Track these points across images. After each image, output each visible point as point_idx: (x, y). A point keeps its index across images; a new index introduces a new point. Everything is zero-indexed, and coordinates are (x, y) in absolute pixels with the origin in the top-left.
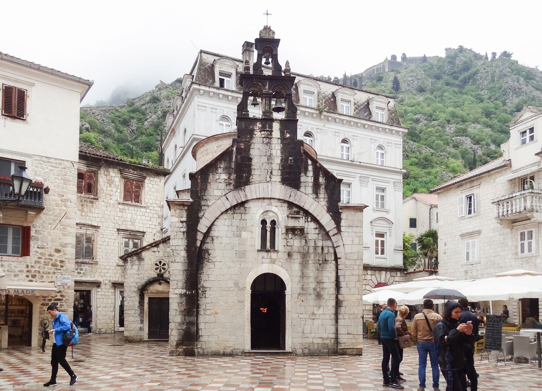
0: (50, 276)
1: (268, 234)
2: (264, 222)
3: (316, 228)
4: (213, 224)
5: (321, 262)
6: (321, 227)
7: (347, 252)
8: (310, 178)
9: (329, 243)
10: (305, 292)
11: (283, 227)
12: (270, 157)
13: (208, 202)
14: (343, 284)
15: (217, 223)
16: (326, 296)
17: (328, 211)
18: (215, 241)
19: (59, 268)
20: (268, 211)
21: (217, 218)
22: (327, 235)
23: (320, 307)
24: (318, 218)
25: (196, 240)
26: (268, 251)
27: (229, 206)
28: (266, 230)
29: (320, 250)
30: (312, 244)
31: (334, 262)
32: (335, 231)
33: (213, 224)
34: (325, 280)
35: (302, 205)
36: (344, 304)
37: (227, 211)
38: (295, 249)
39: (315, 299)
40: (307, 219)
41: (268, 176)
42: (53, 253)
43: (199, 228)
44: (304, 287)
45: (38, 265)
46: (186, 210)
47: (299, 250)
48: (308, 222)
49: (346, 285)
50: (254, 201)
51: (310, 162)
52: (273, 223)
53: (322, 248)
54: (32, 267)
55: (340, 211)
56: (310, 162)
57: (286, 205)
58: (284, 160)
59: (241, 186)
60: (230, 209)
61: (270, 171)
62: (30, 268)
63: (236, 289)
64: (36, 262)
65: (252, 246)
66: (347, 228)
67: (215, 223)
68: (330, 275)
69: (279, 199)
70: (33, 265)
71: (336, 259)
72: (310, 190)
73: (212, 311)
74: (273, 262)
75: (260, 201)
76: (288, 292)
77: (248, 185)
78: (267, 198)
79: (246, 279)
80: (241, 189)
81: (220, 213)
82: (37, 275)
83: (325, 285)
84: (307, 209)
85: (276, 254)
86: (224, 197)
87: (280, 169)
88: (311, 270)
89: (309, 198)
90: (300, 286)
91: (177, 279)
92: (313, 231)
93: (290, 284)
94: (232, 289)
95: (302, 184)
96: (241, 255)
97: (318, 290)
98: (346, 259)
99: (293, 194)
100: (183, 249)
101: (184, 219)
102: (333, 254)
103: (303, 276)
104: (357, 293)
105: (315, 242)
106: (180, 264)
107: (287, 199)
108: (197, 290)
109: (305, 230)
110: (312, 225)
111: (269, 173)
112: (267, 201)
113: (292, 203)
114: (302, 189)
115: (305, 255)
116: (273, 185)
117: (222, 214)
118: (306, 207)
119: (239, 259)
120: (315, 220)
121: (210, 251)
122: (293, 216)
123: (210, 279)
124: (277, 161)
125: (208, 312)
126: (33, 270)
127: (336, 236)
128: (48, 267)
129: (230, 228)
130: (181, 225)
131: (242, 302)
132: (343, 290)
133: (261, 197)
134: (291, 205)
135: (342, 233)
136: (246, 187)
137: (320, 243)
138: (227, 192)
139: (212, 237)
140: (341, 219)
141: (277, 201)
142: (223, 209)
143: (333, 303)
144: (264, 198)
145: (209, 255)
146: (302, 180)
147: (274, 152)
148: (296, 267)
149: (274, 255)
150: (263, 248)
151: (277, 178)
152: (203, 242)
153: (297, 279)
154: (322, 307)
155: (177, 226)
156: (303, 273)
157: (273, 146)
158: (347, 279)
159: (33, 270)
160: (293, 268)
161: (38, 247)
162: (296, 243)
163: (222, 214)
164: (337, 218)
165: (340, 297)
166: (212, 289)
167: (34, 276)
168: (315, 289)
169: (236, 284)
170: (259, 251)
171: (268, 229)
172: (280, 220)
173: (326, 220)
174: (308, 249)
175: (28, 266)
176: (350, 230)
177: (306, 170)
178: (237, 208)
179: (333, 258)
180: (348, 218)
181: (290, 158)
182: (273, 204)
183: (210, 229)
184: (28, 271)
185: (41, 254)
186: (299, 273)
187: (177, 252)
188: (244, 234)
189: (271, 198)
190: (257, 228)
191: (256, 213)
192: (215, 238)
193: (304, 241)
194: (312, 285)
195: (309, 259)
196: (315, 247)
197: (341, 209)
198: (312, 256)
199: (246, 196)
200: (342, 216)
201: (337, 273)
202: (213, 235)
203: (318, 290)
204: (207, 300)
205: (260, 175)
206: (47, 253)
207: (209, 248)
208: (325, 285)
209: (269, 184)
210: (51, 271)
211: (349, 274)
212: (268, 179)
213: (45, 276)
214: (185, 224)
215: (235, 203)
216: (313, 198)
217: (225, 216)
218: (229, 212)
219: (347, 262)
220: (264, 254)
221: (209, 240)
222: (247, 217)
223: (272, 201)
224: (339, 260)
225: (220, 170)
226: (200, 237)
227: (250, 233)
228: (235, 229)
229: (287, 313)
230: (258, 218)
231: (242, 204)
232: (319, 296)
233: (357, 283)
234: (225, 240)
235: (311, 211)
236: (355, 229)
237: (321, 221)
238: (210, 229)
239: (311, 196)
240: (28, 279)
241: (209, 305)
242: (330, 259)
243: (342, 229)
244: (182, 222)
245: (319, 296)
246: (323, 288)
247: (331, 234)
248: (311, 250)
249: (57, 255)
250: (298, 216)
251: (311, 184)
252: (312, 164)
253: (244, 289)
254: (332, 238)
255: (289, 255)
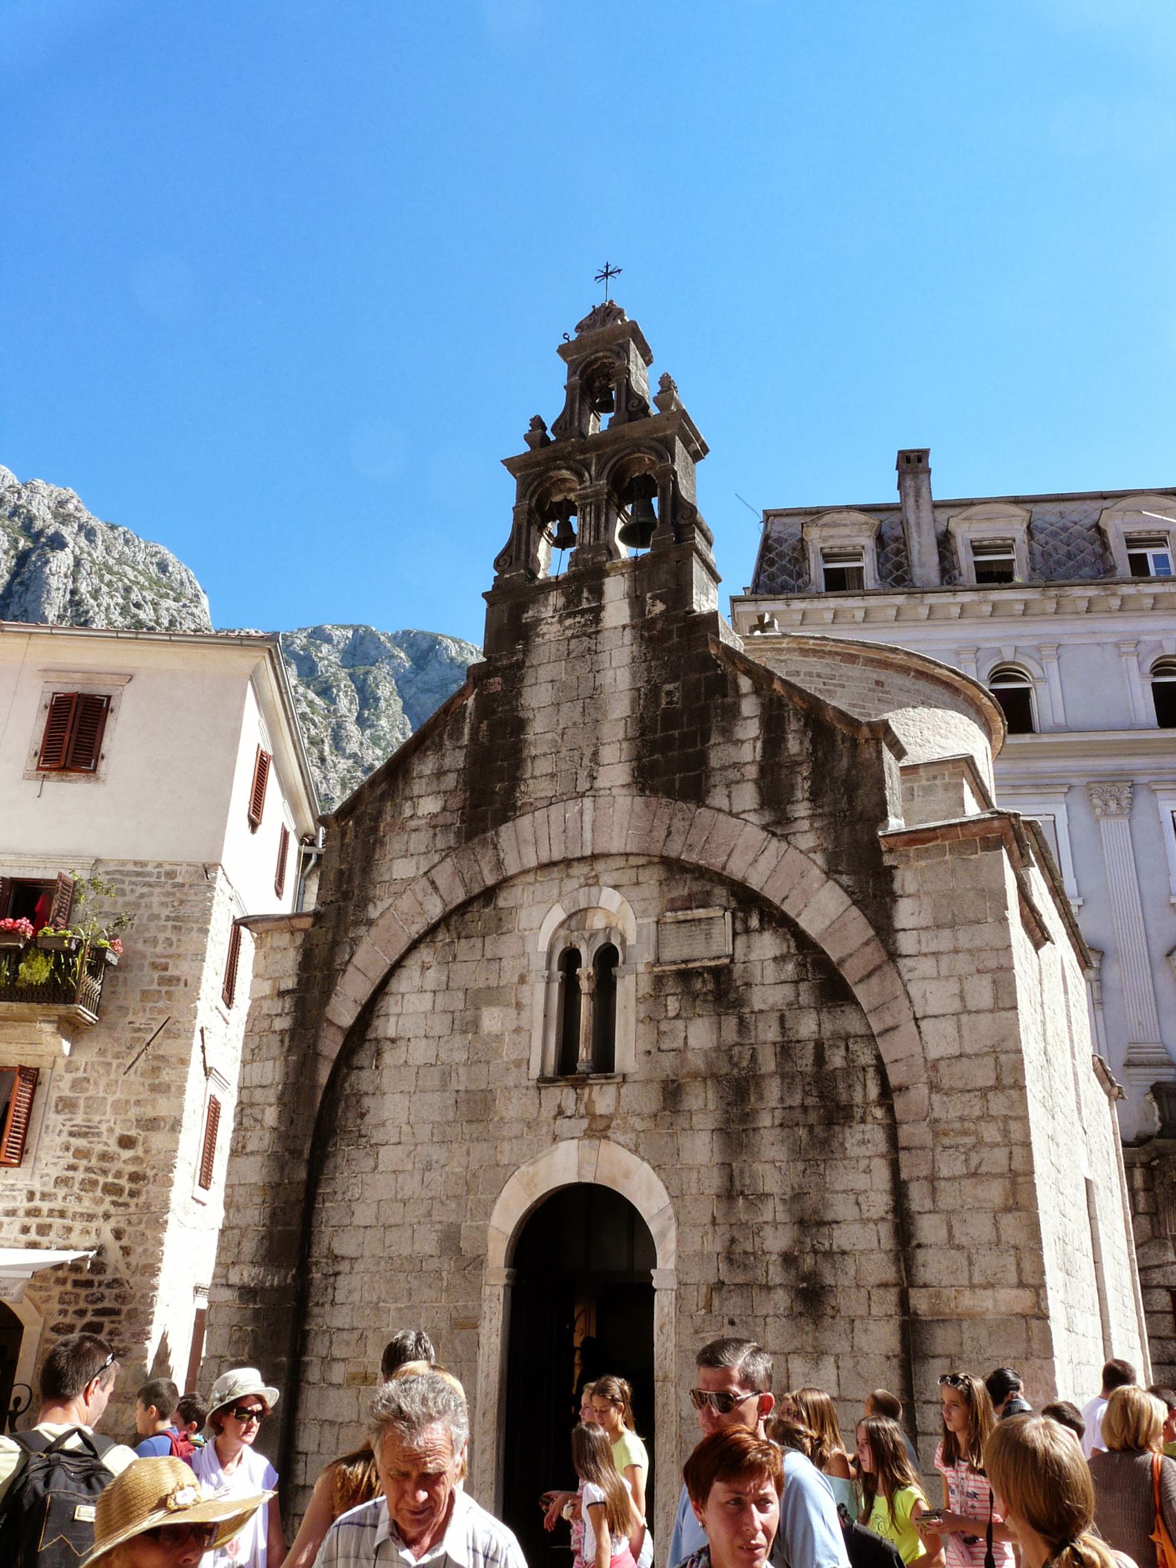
0: (94, 1225)
1: (586, 1006)
2: (570, 958)
3: (779, 960)
4: (381, 990)
5: (813, 1118)
6: (805, 947)
7: (933, 1054)
8: (747, 747)
9: (851, 1022)
10: (740, 1278)
11: (641, 968)
12: (593, 698)
13: (371, 907)
14: (929, 1229)
15: (404, 983)
16: (849, 1302)
17: (831, 872)
18: (388, 1058)
19: (124, 1198)
20: (585, 910)
21: (397, 965)
22: (832, 988)
23: (818, 1355)
24: (785, 908)
25: (317, 1055)
26: (579, 1083)
27: (435, 909)
28: (592, 995)
29: (805, 1061)
30: (769, 1032)
31: (879, 1113)
32: (874, 954)
33: (381, 990)
34: (842, 1208)
35: (716, 862)
36: (942, 1340)
37: (432, 931)
38: (697, 1062)
39: (791, 1316)
40: (745, 921)
41: (583, 774)
42: (113, 1148)
43: (330, 1012)
44: (738, 1249)
45: (61, 1192)
46: (298, 948)
47: (710, 1064)
48: (747, 931)
49: (943, 1233)
50: (530, 878)
51: (745, 684)
52: (607, 957)
53: (819, 1047)
54: (44, 1196)
55: (888, 860)
56: (745, 684)
57: (652, 876)
58: (647, 697)
59: (484, 831)
60: (445, 920)
61: (588, 752)
62: (37, 1203)
63: (447, 1266)
64: (60, 1181)
65: (518, 1064)
66: (924, 935)
67: (394, 986)
68: (860, 1181)
69: (627, 855)
70: (49, 1189)
71: (887, 1094)
72: (747, 796)
73: (352, 1369)
74: (599, 1129)
75: (556, 873)
76: (664, 1275)
77: (506, 820)
78: (581, 859)
79: (488, 1215)
80: (484, 843)
81: (403, 944)
82: (57, 1222)
83: (842, 1238)
84: (738, 875)
85: (611, 1090)
86: (424, 882)
87: (626, 739)
88: (772, 1165)
89: (749, 828)
90: (715, 1245)
91: (242, 1223)
92: (770, 973)
93: (672, 1234)
94: (433, 1264)
95: (716, 778)
96: (477, 1108)
97: (808, 1262)
98: (934, 1087)
99: (678, 824)
100: (273, 1100)
101: (290, 983)
102: (871, 1073)
103: (731, 1192)
104: (1013, 1278)
105: (782, 1019)
106: (259, 1158)
107: (656, 849)
108: (303, 1264)
109: (738, 969)
110: (767, 945)
111: (586, 762)
112: (580, 870)
113: (678, 860)
114: (718, 798)
115: (738, 1090)
116: (601, 801)
117: (414, 946)
118: (737, 868)
119: (467, 1128)
120: (777, 919)
121: (367, 1102)
122: (681, 915)
123: (359, 1220)
124: (619, 707)
125: (338, 1373)
126: (45, 1206)
127: (875, 980)
128: (91, 1194)
129: (440, 996)
130: (276, 1006)
131: (468, 1324)
132: (934, 1265)
133: (557, 856)
134: (673, 867)
135: (902, 963)
136: (503, 828)
137: (807, 1026)
138: (437, 858)
139: (377, 1040)
140: (894, 898)
141: (620, 862)
142: (417, 928)
143: (882, 1337)
144: (567, 862)
145: (362, 1116)
146: (714, 762)
147: (607, 678)
148: (700, 1148)
149: (603, 1099)
150: (566, 1068)
151: (615, 772)
152: (345, 1061)
153: (703, 1211)
154: (829, 1361)
155: (265, 1011)
156: (731, 1178)
157: (605, 657)
158: (948, 1197)
159: (45, 1206)
160: (686, 1157)
161: (71, 1134)
162: (700, 1035)
163: (414, 946)
164: (873, 890)
165: (920, 1302)
166: (359, 1267)
167: (43, 1230)
168: (789, 1260)
169: (450, 1240)
170: (544, 1081)
171: (585, 986)
172: (631, 940)
173: (824, 909)
174: (753, 1058)
175: (31, 1196)
176: (944, 940)
177: (732, 713)
178: (468, 916)
179: (873, 1091)
180: (928, 887)
181: (668, 687)
182: (606, 878)
183: (369, 1010)
184: (30, 1213)
185: (80, 1154)
186: (713, 1182)
187: (256, 1111)
188: (492, 1020)
189: (594, 857)
190: (540, 988)
191: (537, 923)
192: (387, 1046)
193: (731, 1022)
194: (777, 1241)
195: (759, 1106)
196: (785, 1050)
197: (890, 850)
198: (773, 1090)
199: (499, 864)
200: (897, 886)
201: (895, 1168)
202: (380, 1033)
203: (808, 1262)
204: (339, 1318)
205: (553, 776)
206: (99, 1148)
207: (364, 1087)
208: (842, 1238)
209: (588, 802)
210: (100, 1210)
211: (959, 1169)
212: (583, 785)
213: (78, 1226)
214: (288, 1003)
215: (460, 896)
216: (764, 828)
217: (425, 954)
218: (440, 937)
219: (948, 1110)
220: (564, 1096)
221: (364, 1057)
222: (507, 947)
223: (600, 866)
224: (899, 1103)
225: (418, 787)
226: (331, 1046)
227: (512, 1012)
228: (457, 1001)
229: (658, 1385)
230: (543, 945)
231: (489, 895)
232: (811, 1298)
233: (1007, 1220)
234: (420, 1052)
235: (755, 883)
236: (964, 938)
237: (803, 923)
238: (369, 1010)
239: (753, 817)
240: (24, 1238)
241: (346, 1335)
242: (858, 1098)
243: (906, 943)
244: (281, 994)
245: (811, 1298)
246: (829, 1254)
247: (850, 973)
248: (768, 1062)
249: (127, 1154)
250: (701, 913)
251: (752, 772)
252: (757, 691)
253: (479, 1262)
254: (859, 992)
255: (672, 1093)
